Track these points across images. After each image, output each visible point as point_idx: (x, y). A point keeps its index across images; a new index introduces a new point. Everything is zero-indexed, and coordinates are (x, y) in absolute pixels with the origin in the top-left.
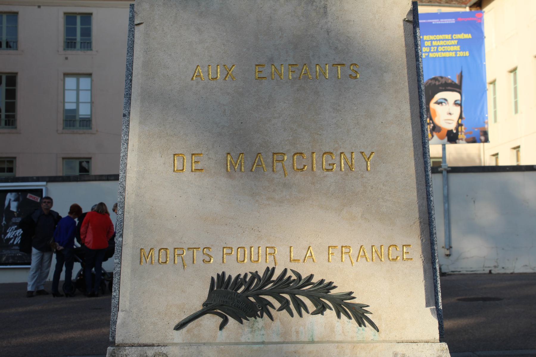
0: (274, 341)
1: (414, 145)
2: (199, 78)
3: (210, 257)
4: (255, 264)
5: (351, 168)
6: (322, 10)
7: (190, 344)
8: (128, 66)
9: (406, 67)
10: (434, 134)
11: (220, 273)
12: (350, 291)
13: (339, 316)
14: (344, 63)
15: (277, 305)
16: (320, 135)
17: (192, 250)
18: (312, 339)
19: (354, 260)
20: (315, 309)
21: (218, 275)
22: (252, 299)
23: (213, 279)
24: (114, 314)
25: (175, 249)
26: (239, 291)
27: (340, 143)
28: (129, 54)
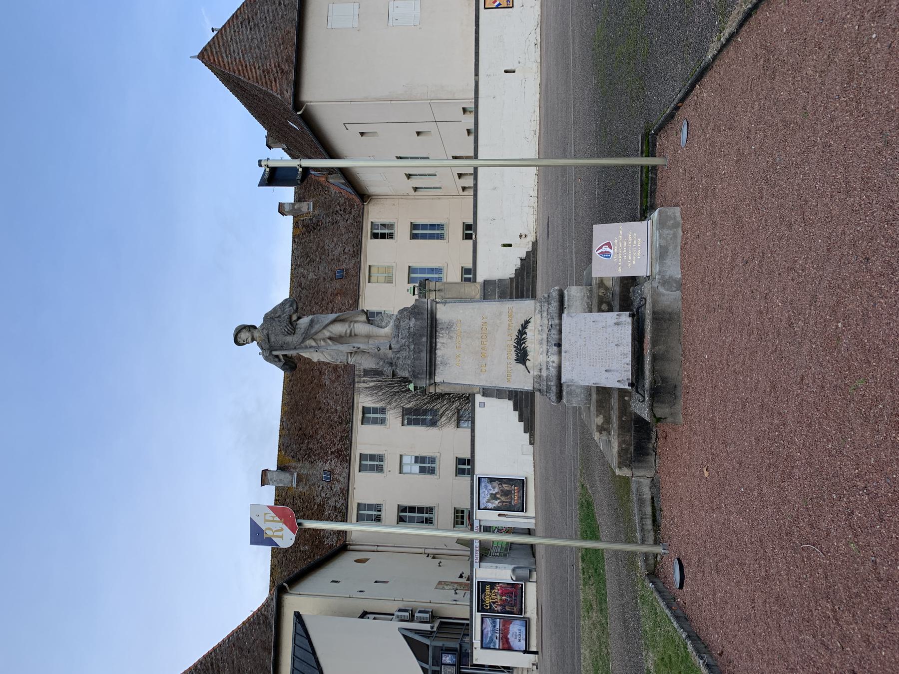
15: (524, 345)
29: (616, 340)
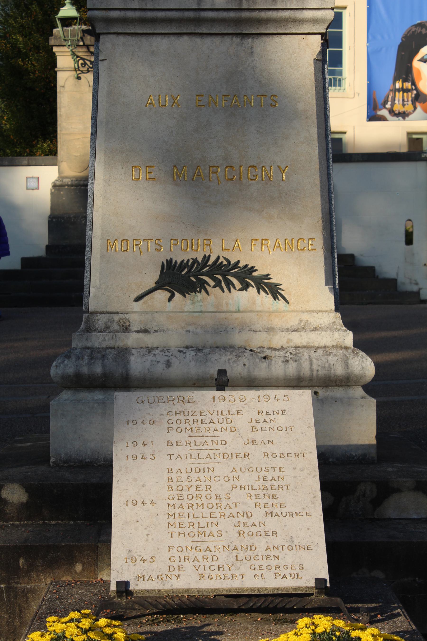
0: (209, 310)
1: (319, 161)
2: (151, 105)
3: (161, 246)
4: (195, 252)
5: (270, 178)
6: (249, 51)
7: (146, 312)
8: (94, 93)
9: (315, 98)
10: (418, 104)
11: (169, 259)
12: (267, 273)
13: (259, 292)
14: (266, 94)
15: (212, 283)
16: (246, 152)
17: (146, 242)
18: (239, 309)
19: (271, 250)
20: (241, 286)
21: (167, 260)
22: (193, 279)
23: (163, 263)
24: (86, 290)
25: (134, 240)
26: (183, 273)
27: (262, 159)
28: (95, 84)
29: (247, 541)
